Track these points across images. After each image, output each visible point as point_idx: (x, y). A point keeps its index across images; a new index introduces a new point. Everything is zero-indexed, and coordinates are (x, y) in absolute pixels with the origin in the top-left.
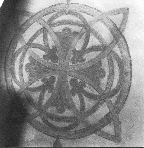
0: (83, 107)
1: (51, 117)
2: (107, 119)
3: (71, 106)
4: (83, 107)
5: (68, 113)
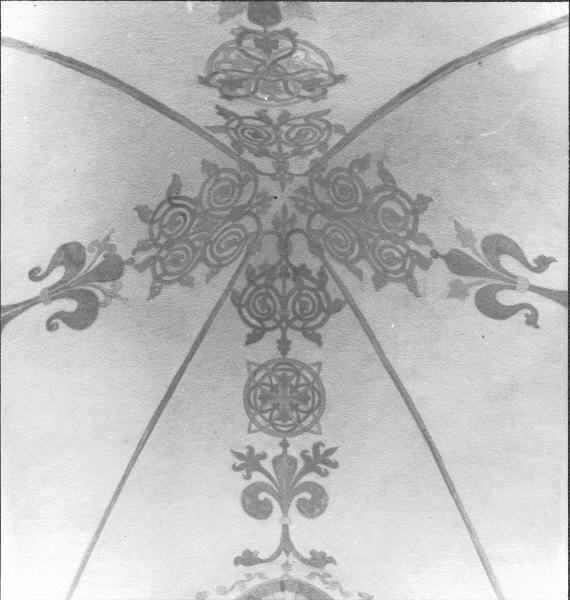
0: (270, 378)
1: (290, 370)
2: (255, 373)
3: (278, 378)
4: (270, 378)
5: (280, 373)
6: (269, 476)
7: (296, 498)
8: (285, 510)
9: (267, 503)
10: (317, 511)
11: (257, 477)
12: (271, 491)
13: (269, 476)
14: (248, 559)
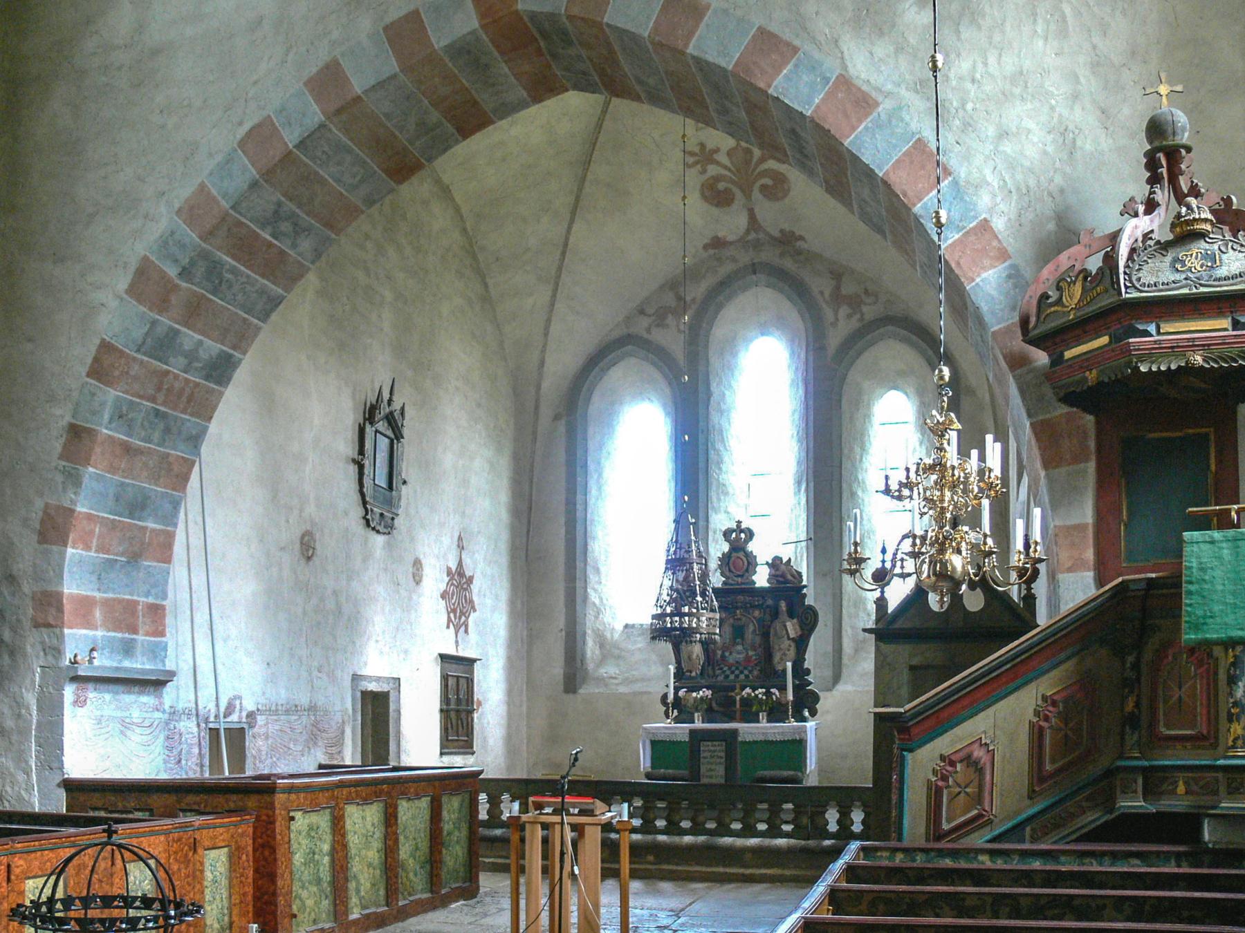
6: (726, 167)
7: (758, 184)
8: (747, 194)
9: (727, 191)
10: (780, 195)
11: (713, 170)
12: (732, 182)
13: (726, 167)
14: (717, 243)
